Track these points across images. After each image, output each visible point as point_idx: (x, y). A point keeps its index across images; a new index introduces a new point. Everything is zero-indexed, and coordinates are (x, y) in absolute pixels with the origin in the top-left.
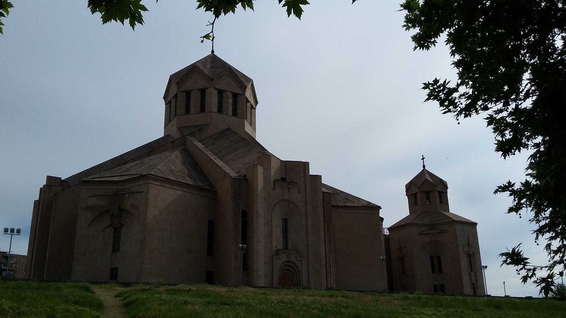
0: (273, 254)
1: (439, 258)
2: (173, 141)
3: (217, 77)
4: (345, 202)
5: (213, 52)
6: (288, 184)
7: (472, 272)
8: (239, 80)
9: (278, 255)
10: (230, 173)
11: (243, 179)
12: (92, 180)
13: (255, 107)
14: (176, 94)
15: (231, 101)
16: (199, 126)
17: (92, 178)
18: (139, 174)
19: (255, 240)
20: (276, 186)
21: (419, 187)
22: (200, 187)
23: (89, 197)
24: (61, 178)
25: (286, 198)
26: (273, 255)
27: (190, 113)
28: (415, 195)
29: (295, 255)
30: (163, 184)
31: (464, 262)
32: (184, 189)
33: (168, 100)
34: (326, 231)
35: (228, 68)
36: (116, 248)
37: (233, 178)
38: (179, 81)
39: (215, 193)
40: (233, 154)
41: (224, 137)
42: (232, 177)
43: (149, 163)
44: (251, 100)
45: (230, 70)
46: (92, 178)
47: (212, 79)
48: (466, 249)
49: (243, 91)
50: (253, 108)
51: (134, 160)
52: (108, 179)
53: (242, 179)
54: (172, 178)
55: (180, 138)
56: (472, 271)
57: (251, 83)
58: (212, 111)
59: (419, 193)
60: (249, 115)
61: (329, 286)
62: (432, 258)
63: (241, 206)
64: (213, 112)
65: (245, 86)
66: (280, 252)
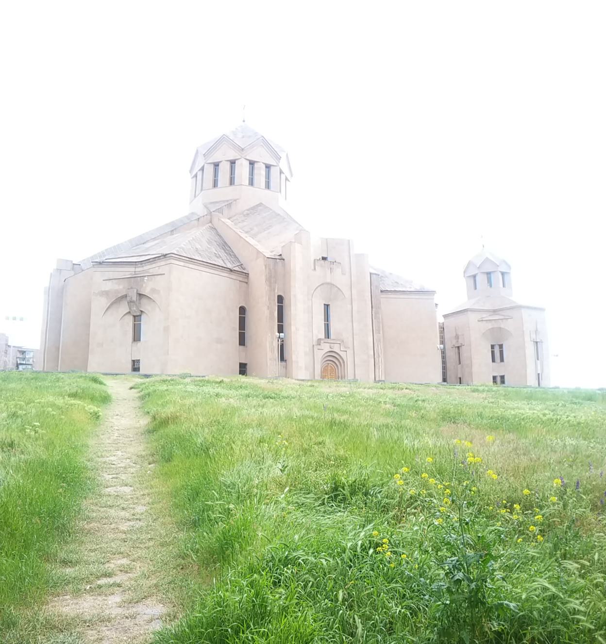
0: (314, 344)
1: (501, 346)
2: (199, 219)
4: (395, 286)
7: (538, 361)
11: (279, 259)
15: (263, 172)
16: (227, 201)
17: (106, 259)
19: (293, 328)
20: (316, 267)
21: (479, 268)
22: (230, 269)
25: (328, 281)
26: (313, 346)
28: (474, 277)
30: (187, 265)
31: (530, 350)
34: (373, 318)
36: (137, 337)
39: (247, 275)
40: (266, 232)
41: (255, 213)
43: (172, 242)
44: (285, 170)
46: (106, 259)
48: (533, 336)
51: (154, 239)
53: (276, 259)
55: (206, 215)
56: (538, 359)
58: (243, 184)
59: (479, 274)
62: (493, 347)
64: (243, 185)
66: (322, 342)
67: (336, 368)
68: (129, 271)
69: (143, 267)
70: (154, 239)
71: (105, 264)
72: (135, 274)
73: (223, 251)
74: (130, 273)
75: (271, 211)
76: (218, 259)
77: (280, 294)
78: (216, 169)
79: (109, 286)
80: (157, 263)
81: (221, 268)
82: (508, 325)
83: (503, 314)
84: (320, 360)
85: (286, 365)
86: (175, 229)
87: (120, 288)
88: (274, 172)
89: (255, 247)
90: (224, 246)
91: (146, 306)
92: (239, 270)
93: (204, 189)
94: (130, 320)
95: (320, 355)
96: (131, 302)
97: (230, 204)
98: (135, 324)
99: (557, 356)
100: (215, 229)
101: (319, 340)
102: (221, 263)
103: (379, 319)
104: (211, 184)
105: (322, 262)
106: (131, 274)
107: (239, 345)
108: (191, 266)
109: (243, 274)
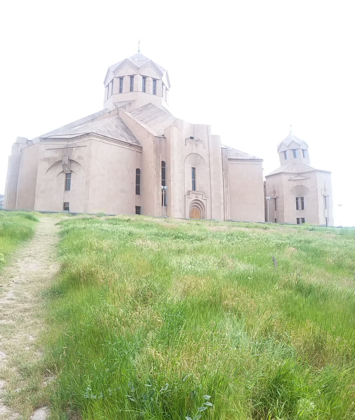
0: (186, 194)
2: (110, 112)
3: (142, 67)
6: (196, 142)
9: (189, 195)
11: (162, 138)
14: (113, 80)
15: (152, 83)
16: (129, 101)
17: (49, 136)
19: (172, 183)
22: (130, 144)
25: (195, 152)
26: (185, 195)
27: (122, 92)
29: (202, 195)
32: (118, 145)
33: (107, 84)
39: (141, 148)
40: (153, 121)
41: (146, 109)
43: (92, 126)
46: (49, 136)
47: (139, 68)
55: (115, 110)
58: (138, 91)
61: (226, 219)
66: (191, 193)
67: (199, 211)
68: (63, 144)
69: (73, 141)
70: (80, 125)
71: (48, 139)
72: (67, 146)
73: (126, 133)
74: (63, 145)
75: (157, 108)
76: (122, 138)
77: (163, 160)
78: (121, 81)
79: (49, 154)
80: (82, 139)
81: (124, 143)
82: (307, 184)
83: (305, 176)
84: (189, 206)
85: (167, 208)
86: (95, 118)
87: (57, 155)
88: (159, 83)
89: (147, 130)
90: (126, 129)
91: (74, 168)
92: (136, 145)
93: (113, 94)
94: (63, 177)
95: (189, 201)
96: (64, 165)
97: (130, 103)
98: (66, 179)
99: (341, 205)
100: (120, 119)
101: (189, 191)
103: (227, 178)
104: (118, 90)
105: (191, 140)
106: (65, 146)
107: (136, 194)
109: (138, 147)
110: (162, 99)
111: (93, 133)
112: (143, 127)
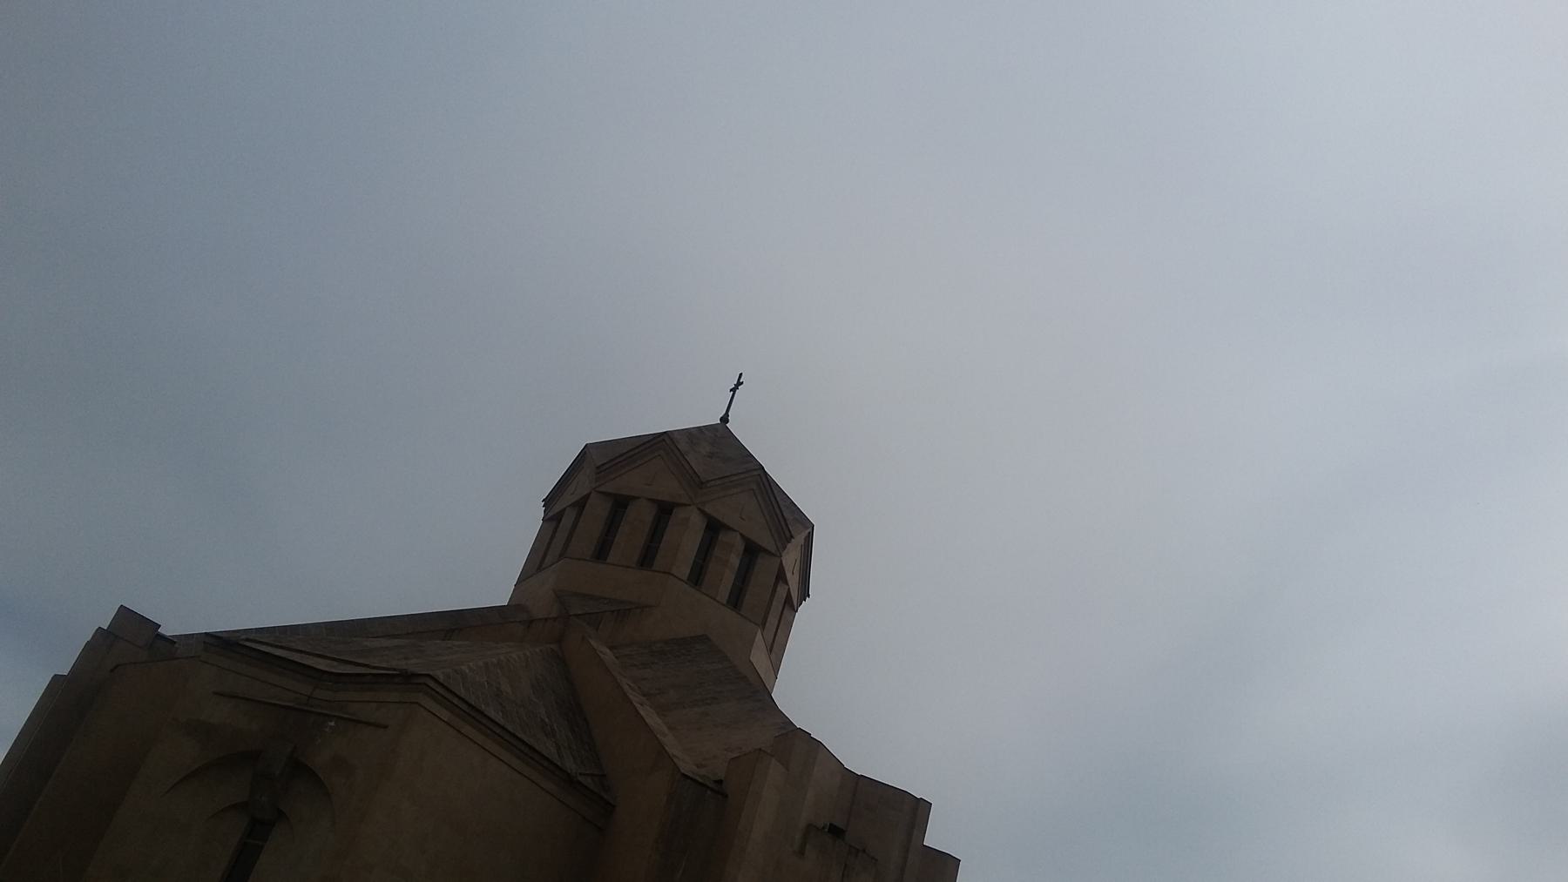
3: (718, 482)
5: (725, 419)
8: (780, 515)
10: (674, 756)
11: (712, 790)
12: (248, 644)
13: (795, 604)
14: (587, 497)
15: (735, 561)
17: (247, 640)
18: (395, 670)
20: (808, 846)
23: (215, 693)
24: (160, 626)
27: (606, 559)
33: (557, 508)
35: (756, 467)
37: (683, 775)
38: (603, 465)
42: (679, 770)
45: (759, 475)
46: (247, 640)
47: (702, 483)
49: (779, 545)
50: (791, 606)
52: (296, 657)
53: (708, 787)
54: (492, 713)
55: (555, 619)
57: (807, 532)
60: (772, 620)
63: (681, 872)
64: (672, 575)
65: (787, 532)
81: (546, 764)
88: (763, 572)
102: (548, 748)
108: (467, 729)
110: (759, 636)
111: (436, 681)
112: (646, 724)
